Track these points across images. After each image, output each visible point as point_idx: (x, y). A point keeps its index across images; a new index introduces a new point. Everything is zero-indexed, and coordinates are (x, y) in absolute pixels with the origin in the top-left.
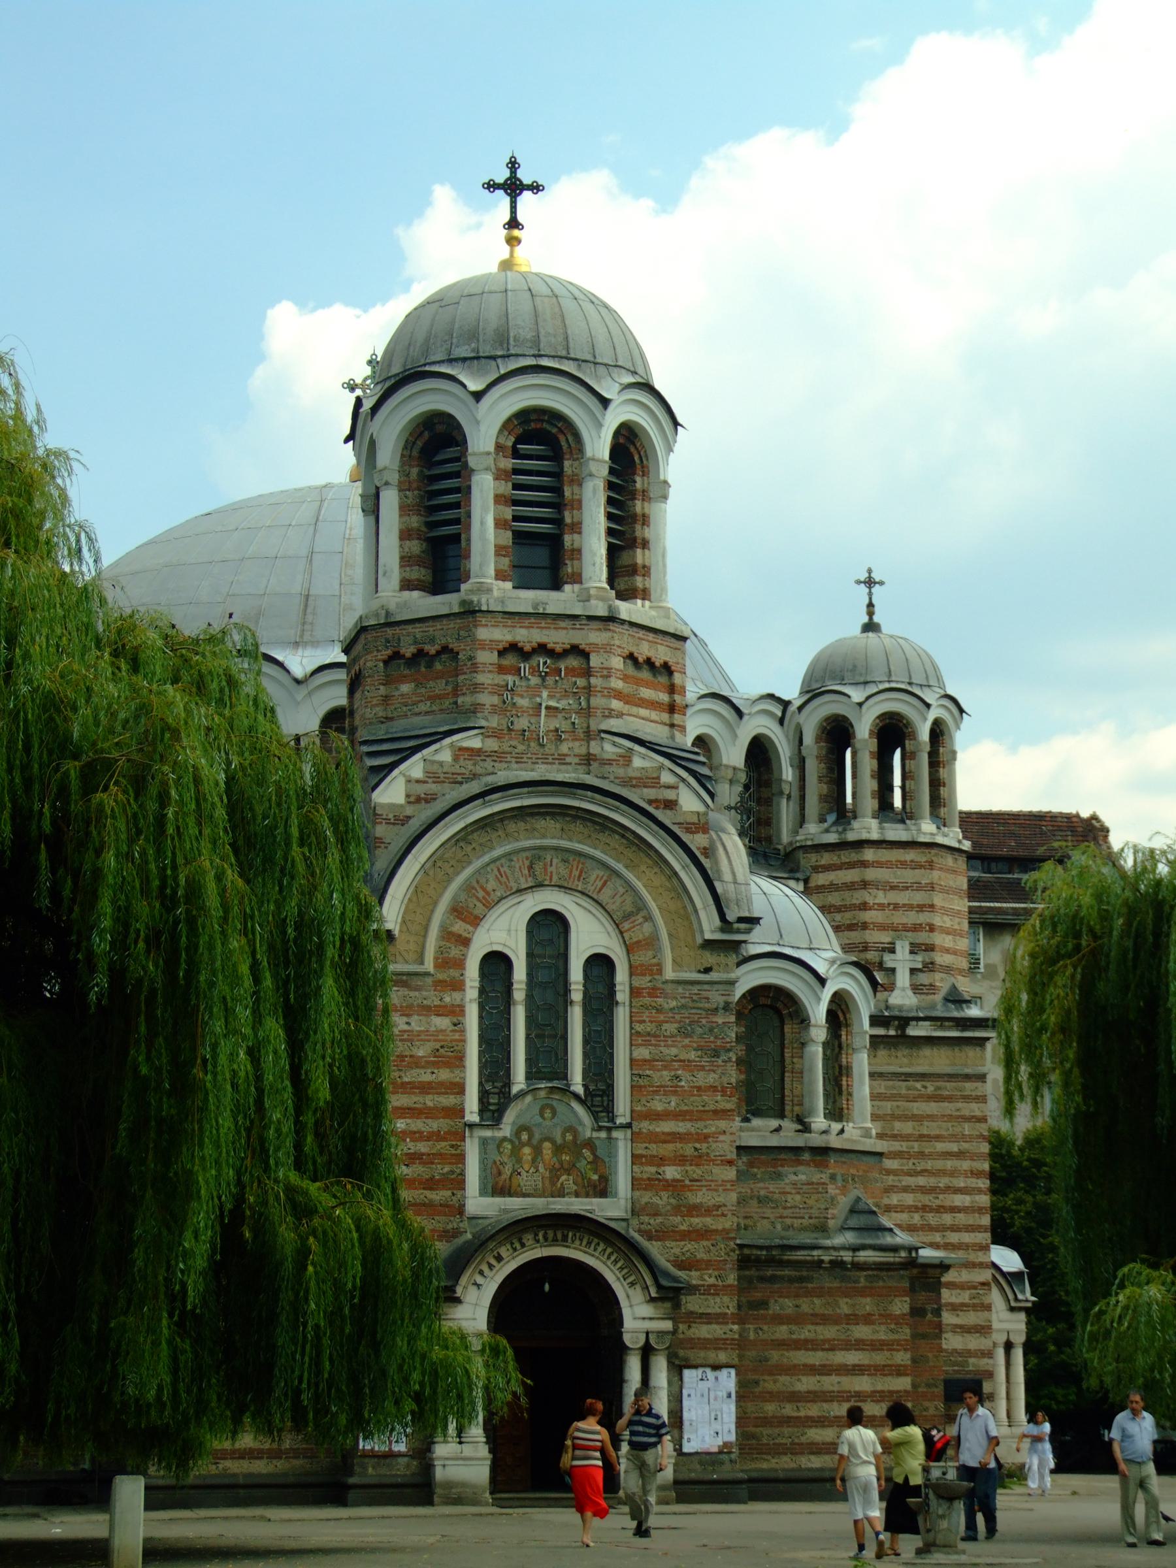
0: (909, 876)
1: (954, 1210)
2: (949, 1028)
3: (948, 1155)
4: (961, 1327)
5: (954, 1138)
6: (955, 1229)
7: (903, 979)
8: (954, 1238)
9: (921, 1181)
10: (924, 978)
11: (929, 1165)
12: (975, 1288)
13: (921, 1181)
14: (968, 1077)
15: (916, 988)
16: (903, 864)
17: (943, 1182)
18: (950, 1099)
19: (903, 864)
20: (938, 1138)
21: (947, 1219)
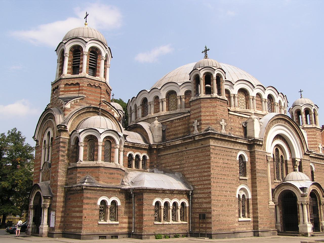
1: (205, 176)
3: (204, 164)
5: (204, 160)
6: (205, 180)
7: (196, 128)
8: (205, 182)
9: (199, 171)
10: (200, 127)
11: (200, 167)
13: (199, 171)
15: (198, 130)
18: (204, 152)
20: (202, 161)
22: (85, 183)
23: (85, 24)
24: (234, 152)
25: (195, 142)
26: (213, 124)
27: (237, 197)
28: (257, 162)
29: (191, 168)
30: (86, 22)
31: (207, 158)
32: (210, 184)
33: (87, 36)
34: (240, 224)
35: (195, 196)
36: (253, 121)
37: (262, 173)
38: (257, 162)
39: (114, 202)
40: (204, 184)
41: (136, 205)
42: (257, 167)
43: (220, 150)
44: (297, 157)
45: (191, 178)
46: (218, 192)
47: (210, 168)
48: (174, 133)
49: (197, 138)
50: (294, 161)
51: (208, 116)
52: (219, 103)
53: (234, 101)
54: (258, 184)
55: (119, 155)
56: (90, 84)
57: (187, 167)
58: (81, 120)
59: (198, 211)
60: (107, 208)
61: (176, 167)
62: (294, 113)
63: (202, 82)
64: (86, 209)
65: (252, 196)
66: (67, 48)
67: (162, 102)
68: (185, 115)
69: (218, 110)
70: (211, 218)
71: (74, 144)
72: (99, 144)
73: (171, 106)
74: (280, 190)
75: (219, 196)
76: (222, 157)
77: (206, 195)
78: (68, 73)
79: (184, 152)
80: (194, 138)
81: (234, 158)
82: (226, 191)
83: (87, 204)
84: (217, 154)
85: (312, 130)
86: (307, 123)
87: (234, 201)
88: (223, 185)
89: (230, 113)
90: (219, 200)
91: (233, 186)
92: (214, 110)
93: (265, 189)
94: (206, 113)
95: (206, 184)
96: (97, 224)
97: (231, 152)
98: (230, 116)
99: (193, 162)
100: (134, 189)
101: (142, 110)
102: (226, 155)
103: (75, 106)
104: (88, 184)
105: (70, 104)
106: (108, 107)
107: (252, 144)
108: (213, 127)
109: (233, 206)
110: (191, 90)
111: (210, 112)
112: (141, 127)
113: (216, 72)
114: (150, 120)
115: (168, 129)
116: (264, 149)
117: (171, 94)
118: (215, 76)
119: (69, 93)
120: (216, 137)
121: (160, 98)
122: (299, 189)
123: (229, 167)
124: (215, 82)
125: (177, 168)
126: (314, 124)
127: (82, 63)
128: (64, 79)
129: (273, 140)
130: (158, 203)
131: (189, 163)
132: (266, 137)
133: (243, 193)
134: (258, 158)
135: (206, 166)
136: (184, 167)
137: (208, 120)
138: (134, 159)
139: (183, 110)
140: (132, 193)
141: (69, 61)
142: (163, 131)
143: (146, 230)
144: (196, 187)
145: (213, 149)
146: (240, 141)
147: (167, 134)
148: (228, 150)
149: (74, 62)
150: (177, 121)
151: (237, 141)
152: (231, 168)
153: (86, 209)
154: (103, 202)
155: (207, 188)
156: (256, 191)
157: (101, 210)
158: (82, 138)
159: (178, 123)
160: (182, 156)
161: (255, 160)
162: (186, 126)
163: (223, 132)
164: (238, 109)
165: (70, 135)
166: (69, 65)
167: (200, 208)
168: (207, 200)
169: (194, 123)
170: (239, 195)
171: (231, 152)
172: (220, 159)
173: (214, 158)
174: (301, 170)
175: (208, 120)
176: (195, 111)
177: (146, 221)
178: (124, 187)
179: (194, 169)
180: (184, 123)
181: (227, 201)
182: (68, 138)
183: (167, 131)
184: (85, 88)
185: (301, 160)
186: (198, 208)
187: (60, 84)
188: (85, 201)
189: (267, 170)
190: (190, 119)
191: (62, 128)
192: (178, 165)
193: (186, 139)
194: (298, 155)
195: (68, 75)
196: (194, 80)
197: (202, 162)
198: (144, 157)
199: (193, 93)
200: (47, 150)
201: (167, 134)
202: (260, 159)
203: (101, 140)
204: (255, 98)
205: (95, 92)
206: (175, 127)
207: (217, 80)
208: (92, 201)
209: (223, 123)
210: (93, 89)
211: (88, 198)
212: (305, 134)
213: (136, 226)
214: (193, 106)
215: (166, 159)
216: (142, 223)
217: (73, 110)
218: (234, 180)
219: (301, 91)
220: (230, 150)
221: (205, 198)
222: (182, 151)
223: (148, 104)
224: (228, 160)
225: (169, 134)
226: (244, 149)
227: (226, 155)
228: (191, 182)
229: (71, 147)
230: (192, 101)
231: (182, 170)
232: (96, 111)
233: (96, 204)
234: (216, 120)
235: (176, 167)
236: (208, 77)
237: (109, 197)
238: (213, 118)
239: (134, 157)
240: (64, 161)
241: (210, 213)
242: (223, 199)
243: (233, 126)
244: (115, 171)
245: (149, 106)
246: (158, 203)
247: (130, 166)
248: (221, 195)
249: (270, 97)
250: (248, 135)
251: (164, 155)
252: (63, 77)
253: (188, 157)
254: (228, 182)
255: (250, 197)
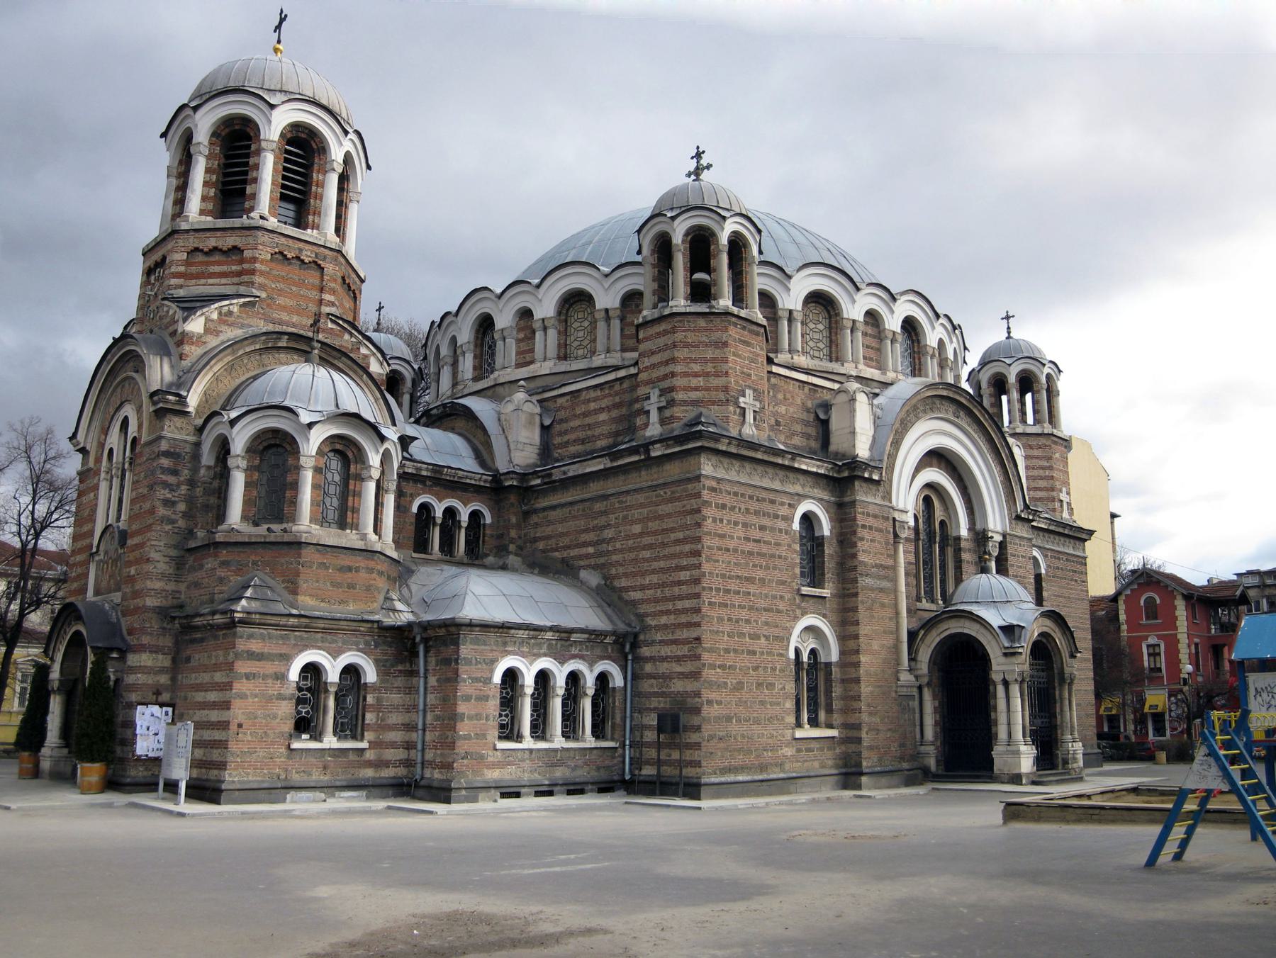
0: (661, 341)
1: (680, 583)
2: (673, 446)
3: (677, 542)
4: (682, 673)
6: (681, 598)
7: (654, 417)
8: (680, 605)
9: (662, 564)
10: (667, 413)
11: (666, 551)
12: (690, 643)
13: (662, 564)
14: (689, 480)
16: (659, 334)
17: (674, 563)
18: (679, 499)
19: (659, 334)
20: (673, 530)
21: (676, 590)
22: (244, 602)
23: (276, 50)
24: (783, 504)
25: (650, 462)
26: (713, 403)
27: (792, 655)
28: (862, 539)
29: (632, 555)
30: (279, 42)
31: (689, 520)
32: (698, 610)
33: (278, 87)
34: (799, 751)
35: (645, 651)
36: (853, 400)
37: (879, 577)
38: (862, 539)
39: (351, 672)
40: (677, 612)
41: (433, 681)
42: (863, 557)
43: (736, 494)
44: (991, 526)
45: (634, 589)
46: (726, 638)
47: (697, 554)
48: (581, 434)
49: (657, 452)
50: (981, 537)
51: (696, 375)
52: (734, 332)
53: (789, 332)
54: (862, 615)
55: (379, 505)
56: (281, 253)
57: (621, 551)
58: (243, 378)
59: (654, 702)
60: (327, 691)
61: (584, 551)
62: (984, 385)
63: (680, 261)
64: (243, 696)
65: (842, 653)
66: (204, 124)
67: (545, 329)
68: (622, 373)
69: (734, 355)
70: (698, 729)
71: (212, 463)
72: (303, 461)
73: (576, 343)
74: (934, 633)
75: (727, 651)
76: (742, 518)
77: (684, 650)
78: (202, 212)
79: (613, 500)
80: (647, 451)
81: (781, 524)
82: (755, 637)
83: (248, 677)
84: (724, 506)
85: (1042, 441)
86: (1024, 421)
87: (782, 671)
88: (744, 614)
89: (775, 369)
90: (730, 667)
91: (776, 618)
92: (718, 354)
93: (885, 632)
94: (693, 365)
95: (684, 611)
96: (283, 750)
97: (773, 502)
98: (773, 380)
99: (641, 535)
100: (426, 626)
101: (475, 357)
102: (756, 513)
103: (223, 328)
104: (255, 606)
105: (202, 319)
106: (347, 337)
107: (847, 479)
108: (713, 412)
109: (778, 686)
110: (641, 288)
111: (706, 361)
112: (469, 414)
113: (730, 227)
114: (500, 390)
115: (562, 421)
116: (887, 496)
117: (576, 300)
118: (724, 239)
119: (203, 281)
120: (724, 448)
121: (538, 315)
122: (998, 631)
123: (764, 555)
124: (725, 258)
125: (588, 556)
126: (1047, 424)
127: (255, 180)
128: (187, 231)
129: (918, 470)
130: (511, 676)
131: (628, 537)
132: (893, 457)
133: (811, 644)
134: (864, 526)
135: (687, 548)
136: (608, 553)
137: (696, 389)
138: (439, 521)
139: (615, 359)
140: (418, 639)
141: (208, 171)
142: (543, 427)
143: (464, 774)
144: (650, 621)
145: (713, 490)
146: (804, 467)
147: (557, 440)
148: (765, 495)
149: (225, 175)
150: (592, 394)
151: (796, 465)
152: (773, 556)
153: (243, 696)
154: (312, 670)
155: (690, 625)
156: (856, 637)
157: (300, 701)
158: (240, 440)
159: (596, 399)
160: (606, 513)
161: (855, 533)
162: (624, 411)
163: (749, 431)
164: (801, 360)
165: (200, 430)
166: (206, 184)
167: (663, 695)
168: (688, 667)
169: (648, 398)
170: (797, 651)
171: (773, 502)
172: (736, 524)
173: (714, 520)
174: (1002, 570)
175: (696, 389)
176: (656, 359)
177: (467, 737)
178: (389, 620)
179: (645, 560)
180: (617, 399)
181: (756, 669)
182: (192, 439)
183: (557, 428)
184: (263, 268)
185: (1004, 536)
186: (656, 694)
187: (171, 251)
188: (242, 667)
189: (894, 568)
190: (634, 388)
191: (168, 402)
192: (590, 544)
193: (620, 454)
194: (996, 521)
195: (203, 218)
196: (653, 252)
197: (672, 535)
198: (475, 515)
199: (648, 299)
200: (116, 482)
201: (557, 440)
202: (871, 528)
203: (311, 444)
204: (861, 327)
205: (301, 284)
206: (585, 415)
207: (730, 254)
208: (270, 668)
209: (747, 400)
210: (294, 271)
211: (252, 656)
212: (1018, 453)
213: (429, 755)
214: (646, 339)
215: (550, 523)
216: (452, 745)
217: (213, 342)
218: (782, 597)
219: (1008, 317)
220: (772, 496)
221: (679, 659)
222: (606, 497)
223: (496, 336)
224: (762, 528)
225: (566, 438)
226: (818, 492)
227: (756, 513)
228: (634, 603)
229: (202, 471)
230: (646, 324)
231: (602, 560)
232: (300, 346)
233: (282, 677)
234: (726, 389)
235: (584, 551)
236: (701, 242)
237: (335, 654)
238: (715, 382)
239: (439, 514)
240: (173, 522)
241: (697, 711)
242: (744, 661)
243: (783, 416)
244: (360, 562)
245: (500, 344)
246: (511, 676)
247: (421, 544)
248: (735, 651)
249: (910, 326)
250: (832, 448)
251: (545, 509)
252: (184, 226)
253: (625, 517)
254: (762, 603)
255: (834, 657)
